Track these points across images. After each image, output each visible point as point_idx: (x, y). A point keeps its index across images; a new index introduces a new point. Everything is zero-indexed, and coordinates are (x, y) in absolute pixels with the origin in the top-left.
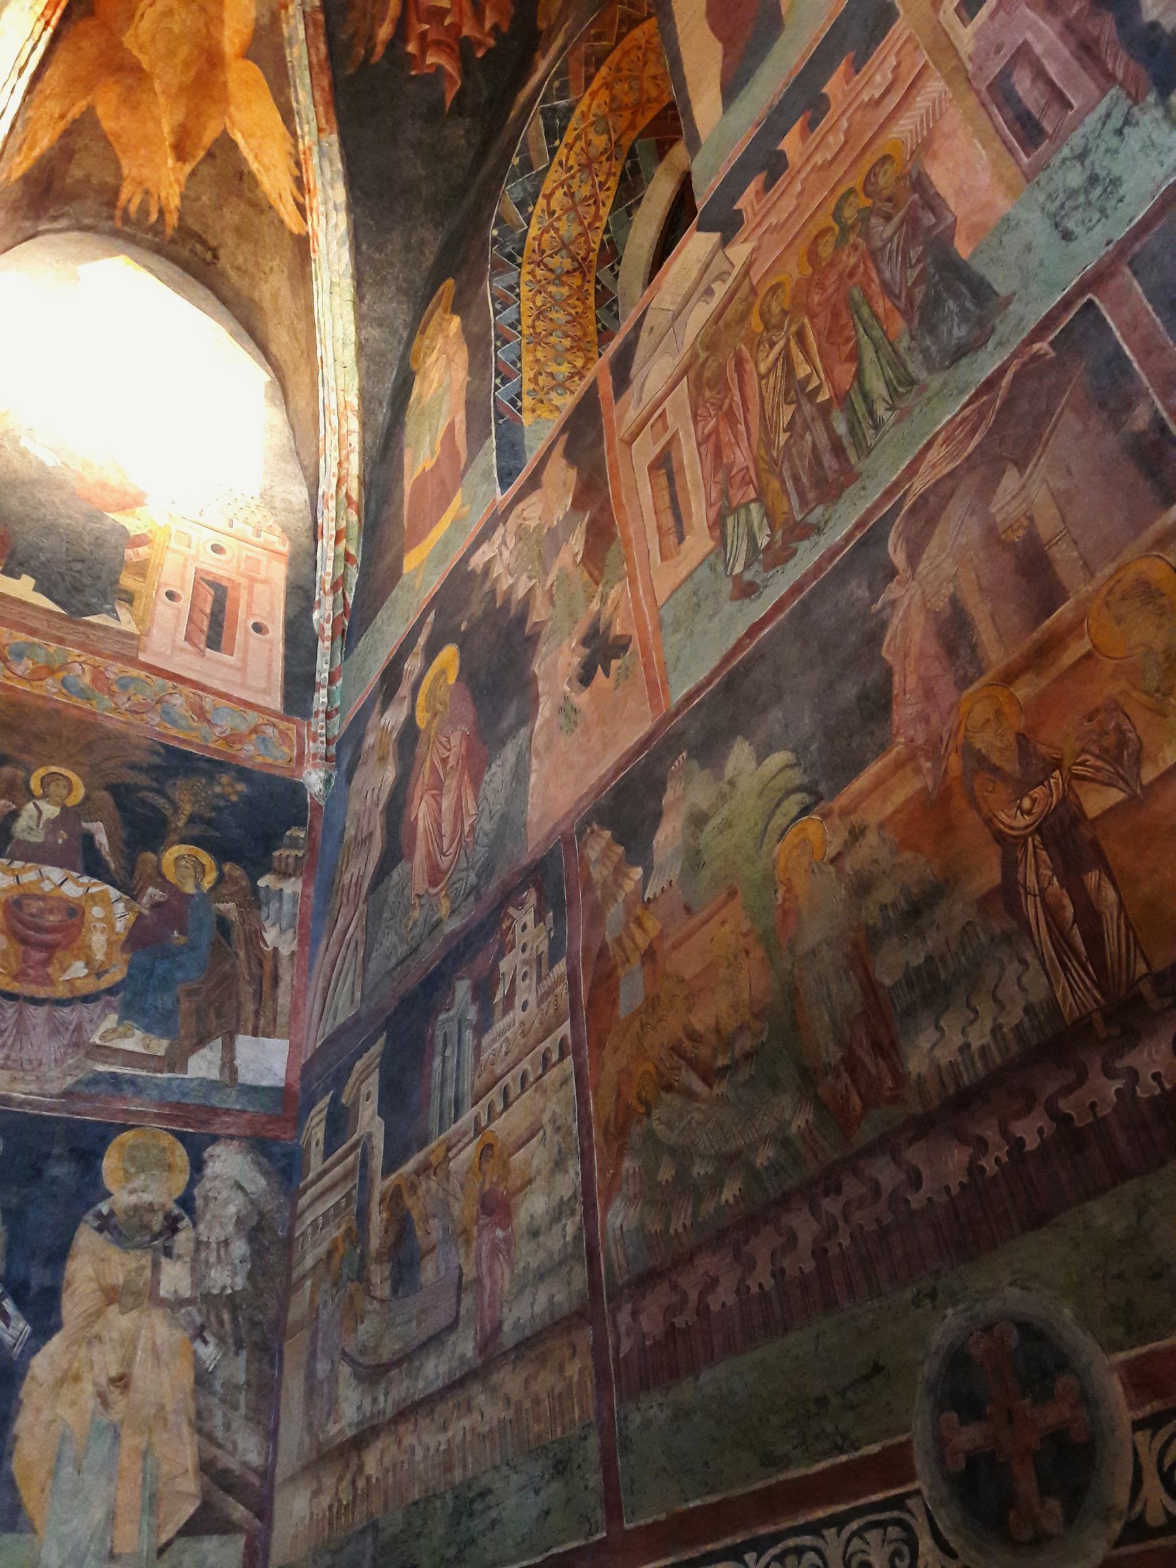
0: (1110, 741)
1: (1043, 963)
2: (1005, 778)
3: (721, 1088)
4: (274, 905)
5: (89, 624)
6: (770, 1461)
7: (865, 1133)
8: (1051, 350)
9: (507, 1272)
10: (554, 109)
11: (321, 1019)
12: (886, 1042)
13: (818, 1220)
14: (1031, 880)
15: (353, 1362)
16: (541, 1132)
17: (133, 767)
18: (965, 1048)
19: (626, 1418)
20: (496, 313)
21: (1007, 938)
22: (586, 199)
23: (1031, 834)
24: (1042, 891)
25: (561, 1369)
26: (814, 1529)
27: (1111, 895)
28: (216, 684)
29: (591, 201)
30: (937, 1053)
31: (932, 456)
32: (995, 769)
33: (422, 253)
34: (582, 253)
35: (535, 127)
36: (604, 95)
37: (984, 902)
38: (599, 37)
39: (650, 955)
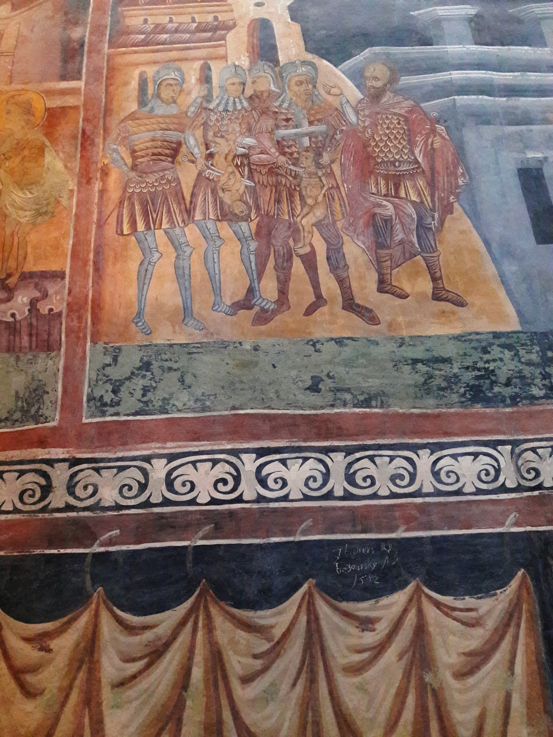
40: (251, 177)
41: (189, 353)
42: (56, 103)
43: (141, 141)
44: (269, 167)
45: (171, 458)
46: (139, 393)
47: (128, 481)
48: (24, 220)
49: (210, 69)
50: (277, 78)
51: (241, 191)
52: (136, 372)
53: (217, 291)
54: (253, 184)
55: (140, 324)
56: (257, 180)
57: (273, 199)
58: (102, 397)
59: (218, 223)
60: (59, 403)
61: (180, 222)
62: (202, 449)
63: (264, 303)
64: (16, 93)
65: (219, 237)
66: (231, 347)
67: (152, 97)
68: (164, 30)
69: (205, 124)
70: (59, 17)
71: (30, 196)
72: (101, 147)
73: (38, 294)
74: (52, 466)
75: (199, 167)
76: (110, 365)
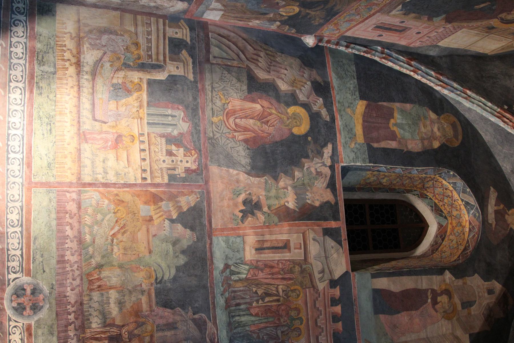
3: (110, 238)
4: (268, 24)
5: (399, 5)
9: (99, 146)
10: (472, 209)
11: (220, 35)
13: (73, 263)
14: (112, 330)
15: (101, 59)
16: (127, 166)
17: (335, 5)
20: (417, 170)
21: (105, 322)
22: (443, 199)
26: (22, 249)
28: (360, 25)
29: (442, 200)
33: (483, 132)
34: (428, 190)
35: (472, 200)
36: (464, 224)
38: (474, 235)
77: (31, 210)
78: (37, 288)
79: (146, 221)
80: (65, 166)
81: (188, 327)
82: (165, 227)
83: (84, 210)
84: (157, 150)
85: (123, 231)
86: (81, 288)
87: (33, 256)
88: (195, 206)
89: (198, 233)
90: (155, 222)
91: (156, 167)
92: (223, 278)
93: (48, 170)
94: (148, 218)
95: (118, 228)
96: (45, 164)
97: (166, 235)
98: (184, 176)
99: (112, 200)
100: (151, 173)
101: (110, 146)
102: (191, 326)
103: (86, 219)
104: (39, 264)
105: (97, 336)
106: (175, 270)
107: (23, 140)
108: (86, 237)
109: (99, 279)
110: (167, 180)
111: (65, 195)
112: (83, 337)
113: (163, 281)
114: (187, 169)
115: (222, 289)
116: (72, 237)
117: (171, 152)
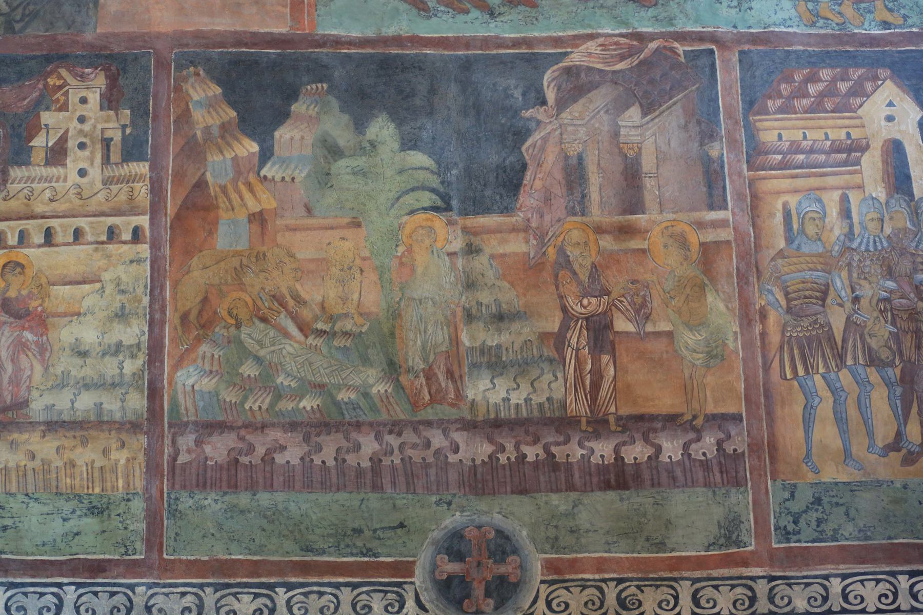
0: (639, 300)
1: (566, 383)
2: (580, 283)
3: (310, 340)
6: (308, 549)
7: (429, 414)
8: (682, 56)
9: (38, 368)
12: (457, 375)
14: (574, 341)
16: (98, 285)
18: (507, 400)
19: (177, 499)
21: (551, 361)
23: (582, 318)
24: (578, 350)
25: (105, 452)
26: (337, 586)
27: (612, 371)
30: (487, 394)
31: (591, 46)
32: (575, 273)
37: (544, 337)
39: (259, 219)
40: (894, 323)
41: (852, 491)
42: (710, 236)
43: (794, 282)
44: (909, 312)
45: (844, 577)
46: (814, 524)
47: (814, 594)
48: (698, 363)
49: (849, 202)
50: (912, 214)
51: (886, 337)
52: (810, 506)
53: (870, 434)
54: (896, 330)
55: (810, 464)
56: (899, 326)
57: (913, 345)
58: (785, 527)
59: (867, 368)
60: (753, 531)
61: (834, 367)
62: (866, 570)
63: (910, 447)
64: (669, 224)
65: (868, 382)
66: (885, 486)
67: (798, 233)
68: (799, 151)
69: (849, 265)
70: (694, 129)
71: (700, 338)
72: (756, 286)
73: (722, 436)
74: (755, 582)
75: (847, 310)
76: (788, 500)
77: (226, 560)
78: (446, 545)
79: (263, 234)
80: (97, 464)
81: (579, 122)
82: (283, 178)
83: (229, 411)
84: (48, 194)
85: (291, 303)
86: (450, 426)
87: (356, 555)
88: (219, 83)
89: (305, 79)
90: (266, 206)
91: (101, 197)
92: (442, 8)
93: (109, 516)
94: (256, 228)
95: (282, 316)
96: (90, 523)
97: (308, 175)
98: (128, 112)
99: (201, 332)
100: (118, 213)
101: (36, 336)
102: (577, 114)
103: (255, 407)
104: (379, 539)
105: (588, 382)
106: (411, 152)
107: (23, 585)
108: (309, 408)
109: (429, 375)
110: (141, 164)
111: (184, 466)
112: (588, 422)
113: (442, 190)
114: (106, 105)
115: (475, 13)
116: (306, 449)
117: (52, 149)
